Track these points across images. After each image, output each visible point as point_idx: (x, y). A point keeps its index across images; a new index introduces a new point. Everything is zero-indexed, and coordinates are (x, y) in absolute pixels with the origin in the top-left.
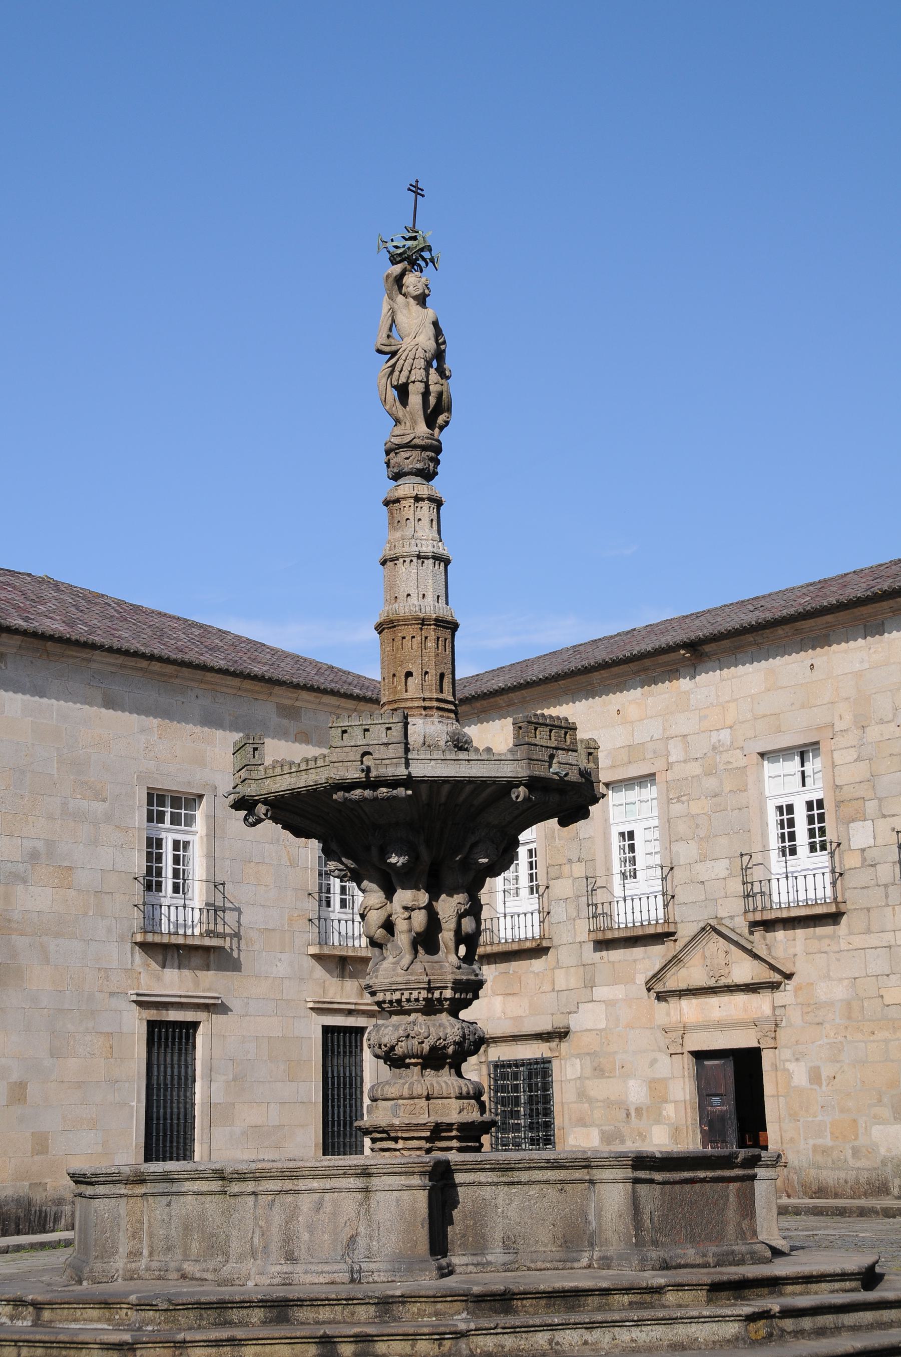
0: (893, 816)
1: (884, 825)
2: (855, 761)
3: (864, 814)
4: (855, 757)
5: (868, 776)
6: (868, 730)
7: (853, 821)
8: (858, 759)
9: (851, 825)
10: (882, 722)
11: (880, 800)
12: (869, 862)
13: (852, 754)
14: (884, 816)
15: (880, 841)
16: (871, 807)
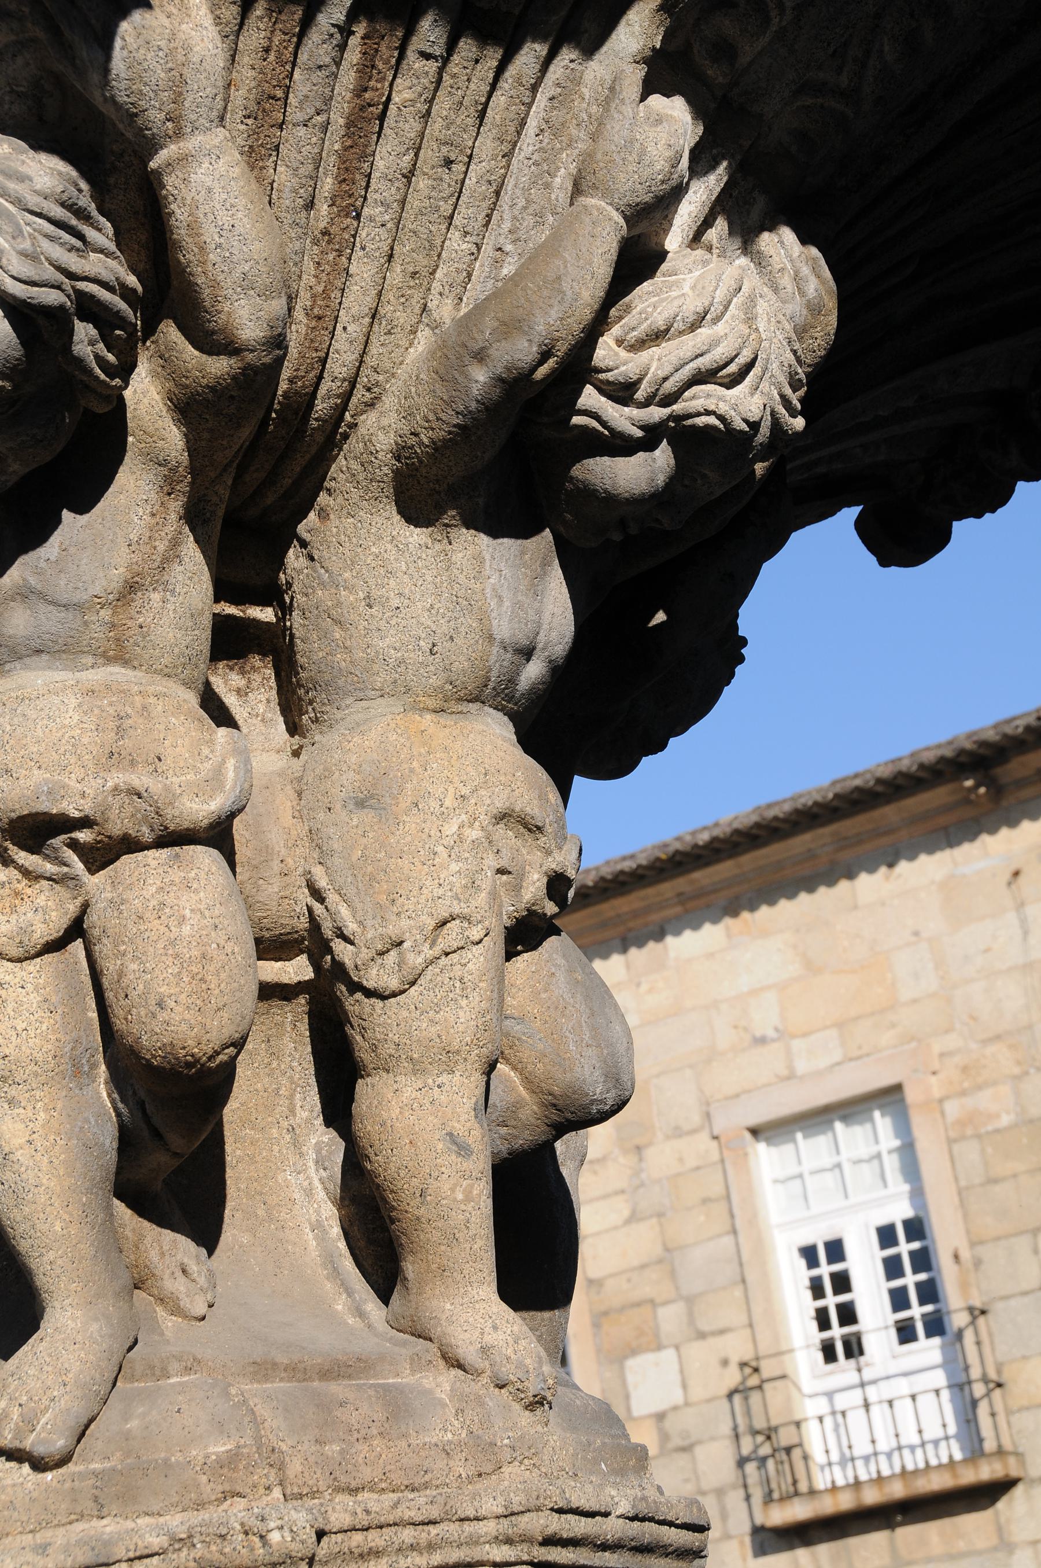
0: (722, 1332)
1: (699, 1353)
2: (628, 1221)
3: (657, 1335)
4: (626, 1213)
5: (658, 1250)
6: (649, 1153)
7: (634, 1352)
8: (634, 1218)
9: (631, 1363)
10: (678, 1133)
11: (690, 1301)
12: (676, 1441)
13: (621, 1208)
14: (702, 1336)
15: (697, 1393)
16: (670, 1318)
